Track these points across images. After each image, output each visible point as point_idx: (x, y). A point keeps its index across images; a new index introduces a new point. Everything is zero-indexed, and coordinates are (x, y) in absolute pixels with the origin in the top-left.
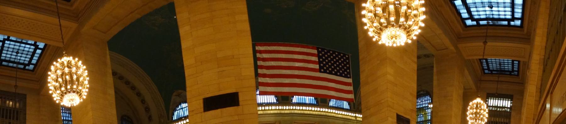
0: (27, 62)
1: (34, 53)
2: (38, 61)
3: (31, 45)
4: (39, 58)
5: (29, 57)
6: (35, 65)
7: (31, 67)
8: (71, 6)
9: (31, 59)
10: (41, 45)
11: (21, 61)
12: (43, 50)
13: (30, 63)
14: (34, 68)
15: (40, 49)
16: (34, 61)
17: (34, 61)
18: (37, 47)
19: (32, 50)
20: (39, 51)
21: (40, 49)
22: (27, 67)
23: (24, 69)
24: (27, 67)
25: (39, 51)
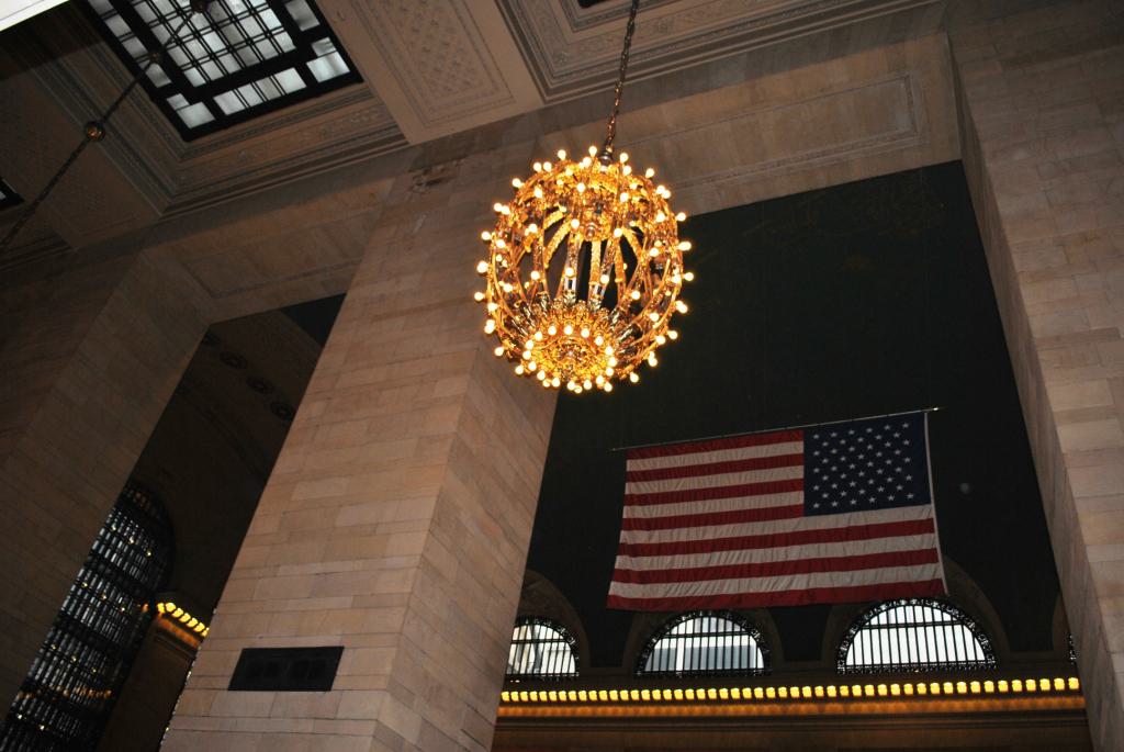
0: (195, 77)
1: (269, 68)
2: (249, 113)
3: (289, 24)
4: (267, 107)
5: (231, 65)
6: (221, 120)
7: (196, 114)
8: (577, 26)
9: (230, 82)
10: (325, 66)
11: (179, 56)
12: (314, 88)
13: (206, 94)
14: (203, 130)
15: (306, 75)
16: (229, 102)
17: (229, 102)
18: (299, 58)
19: (267, 50)
20: (290, 80)
21: (306, 75)
22: (178, 100)
23: (160, 96)
24: (178, 100)
25: (290, 80)
